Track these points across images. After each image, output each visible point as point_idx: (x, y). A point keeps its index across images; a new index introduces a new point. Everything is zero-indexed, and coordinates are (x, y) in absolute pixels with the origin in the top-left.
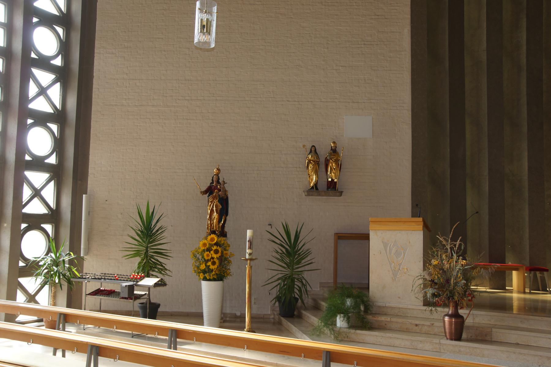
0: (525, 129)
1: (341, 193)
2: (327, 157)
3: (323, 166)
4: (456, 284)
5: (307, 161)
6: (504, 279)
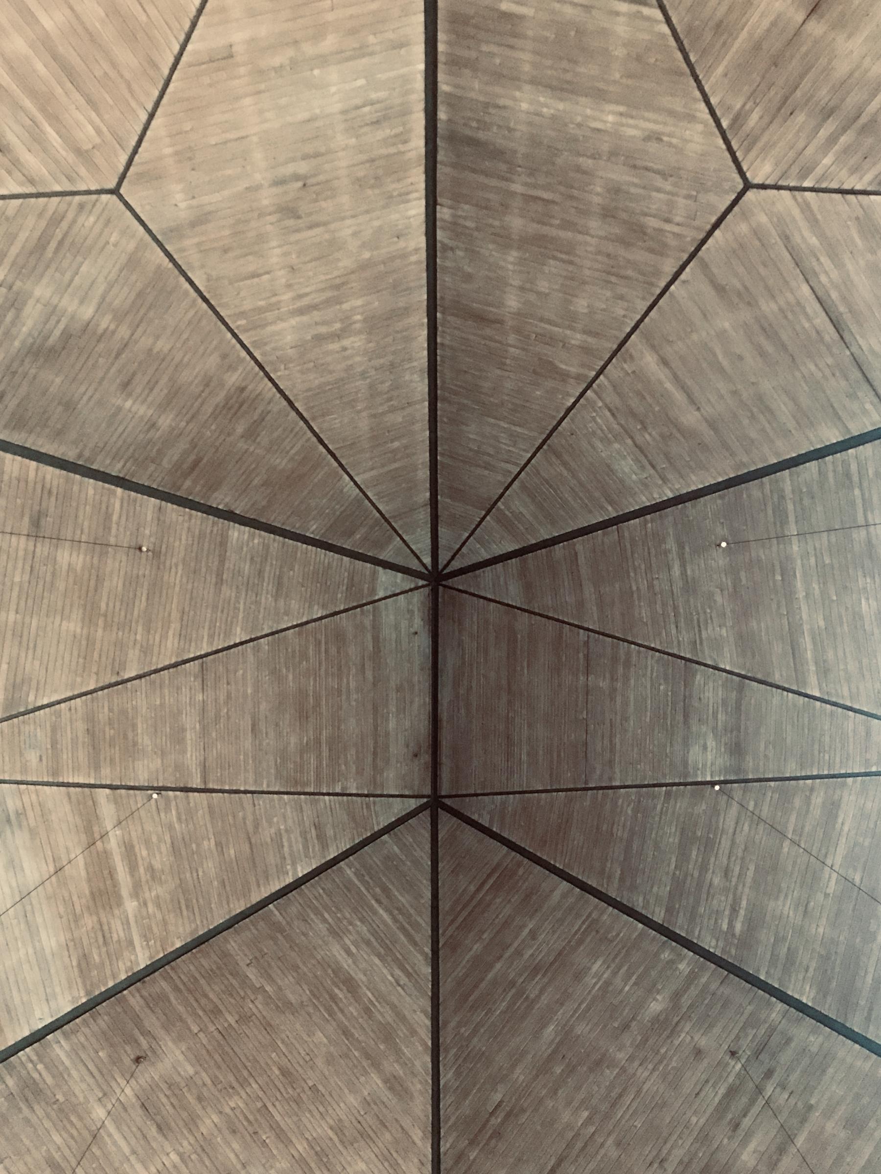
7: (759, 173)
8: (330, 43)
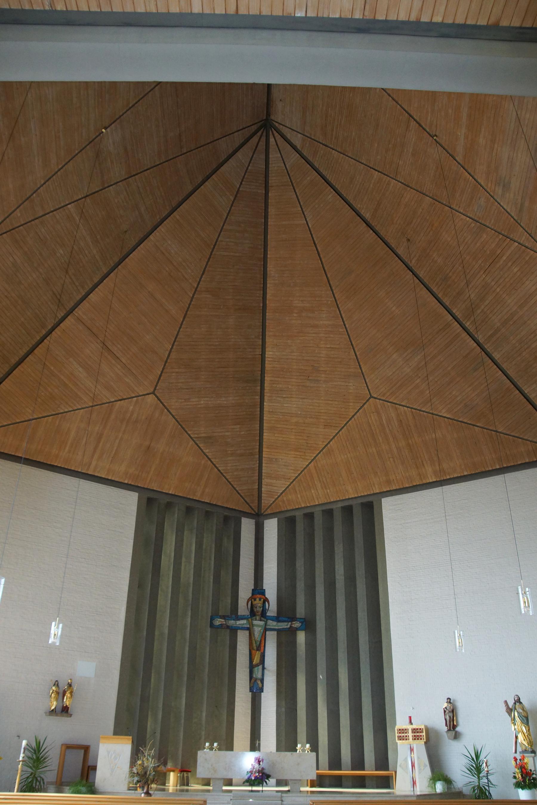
0: (185, 679)
1: (71, 715)
2: (65, 689)
3: (61, 695)
4: (150, 774)
5: (51, 691)
6: (165, 778)
7: (151, 399)
8: (294, 420)
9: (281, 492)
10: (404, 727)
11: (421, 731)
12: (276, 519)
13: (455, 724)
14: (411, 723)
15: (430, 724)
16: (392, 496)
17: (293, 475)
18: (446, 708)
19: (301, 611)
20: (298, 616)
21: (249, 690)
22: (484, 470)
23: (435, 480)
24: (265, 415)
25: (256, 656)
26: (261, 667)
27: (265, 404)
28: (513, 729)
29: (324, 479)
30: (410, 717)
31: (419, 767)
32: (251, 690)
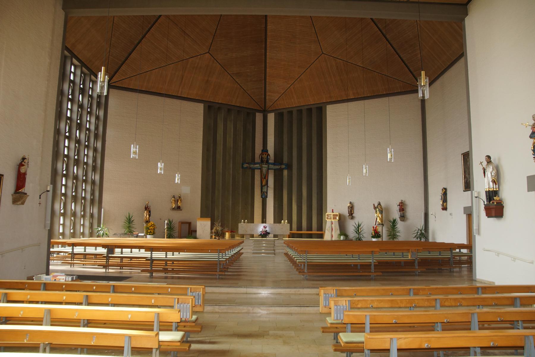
1: (181, 210)
3: (176, 202)
9: (276, 99)
10: (330, 214)
11: (337, 215)
12: (274, 113)
13: (352, 213)
14: (333, 212)
15: (341, 213)
16: (332, 104)
17: (282, 91)
18: (349, 206)
19: (285, 160)
20: (284, 162)
21: (261, 197)
22: (378, 94)
23: (353, 98)
24: (267, 60)
25: (264, 182)
26: (266, 186)
27: (267, 54)
28: (376, 216)
29: (298, 94)
30: (333, 210)
31: (335, 229)
32: (262, 197)
